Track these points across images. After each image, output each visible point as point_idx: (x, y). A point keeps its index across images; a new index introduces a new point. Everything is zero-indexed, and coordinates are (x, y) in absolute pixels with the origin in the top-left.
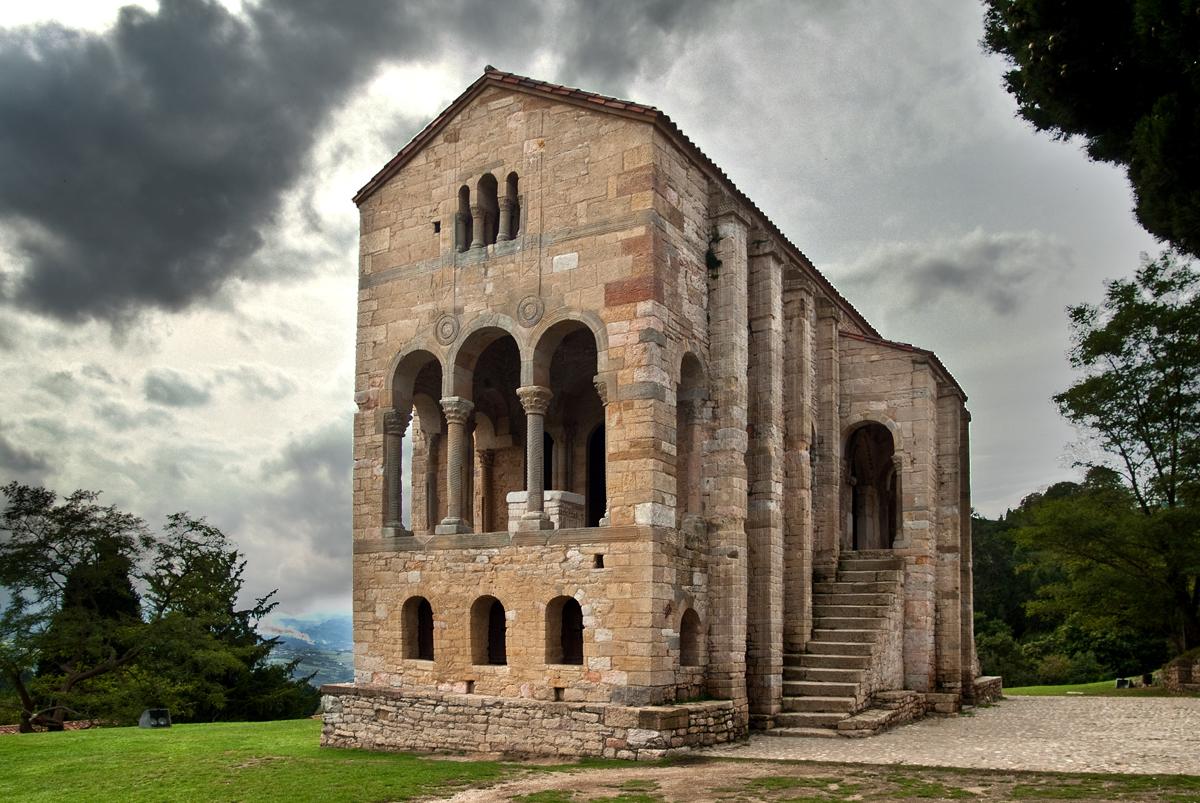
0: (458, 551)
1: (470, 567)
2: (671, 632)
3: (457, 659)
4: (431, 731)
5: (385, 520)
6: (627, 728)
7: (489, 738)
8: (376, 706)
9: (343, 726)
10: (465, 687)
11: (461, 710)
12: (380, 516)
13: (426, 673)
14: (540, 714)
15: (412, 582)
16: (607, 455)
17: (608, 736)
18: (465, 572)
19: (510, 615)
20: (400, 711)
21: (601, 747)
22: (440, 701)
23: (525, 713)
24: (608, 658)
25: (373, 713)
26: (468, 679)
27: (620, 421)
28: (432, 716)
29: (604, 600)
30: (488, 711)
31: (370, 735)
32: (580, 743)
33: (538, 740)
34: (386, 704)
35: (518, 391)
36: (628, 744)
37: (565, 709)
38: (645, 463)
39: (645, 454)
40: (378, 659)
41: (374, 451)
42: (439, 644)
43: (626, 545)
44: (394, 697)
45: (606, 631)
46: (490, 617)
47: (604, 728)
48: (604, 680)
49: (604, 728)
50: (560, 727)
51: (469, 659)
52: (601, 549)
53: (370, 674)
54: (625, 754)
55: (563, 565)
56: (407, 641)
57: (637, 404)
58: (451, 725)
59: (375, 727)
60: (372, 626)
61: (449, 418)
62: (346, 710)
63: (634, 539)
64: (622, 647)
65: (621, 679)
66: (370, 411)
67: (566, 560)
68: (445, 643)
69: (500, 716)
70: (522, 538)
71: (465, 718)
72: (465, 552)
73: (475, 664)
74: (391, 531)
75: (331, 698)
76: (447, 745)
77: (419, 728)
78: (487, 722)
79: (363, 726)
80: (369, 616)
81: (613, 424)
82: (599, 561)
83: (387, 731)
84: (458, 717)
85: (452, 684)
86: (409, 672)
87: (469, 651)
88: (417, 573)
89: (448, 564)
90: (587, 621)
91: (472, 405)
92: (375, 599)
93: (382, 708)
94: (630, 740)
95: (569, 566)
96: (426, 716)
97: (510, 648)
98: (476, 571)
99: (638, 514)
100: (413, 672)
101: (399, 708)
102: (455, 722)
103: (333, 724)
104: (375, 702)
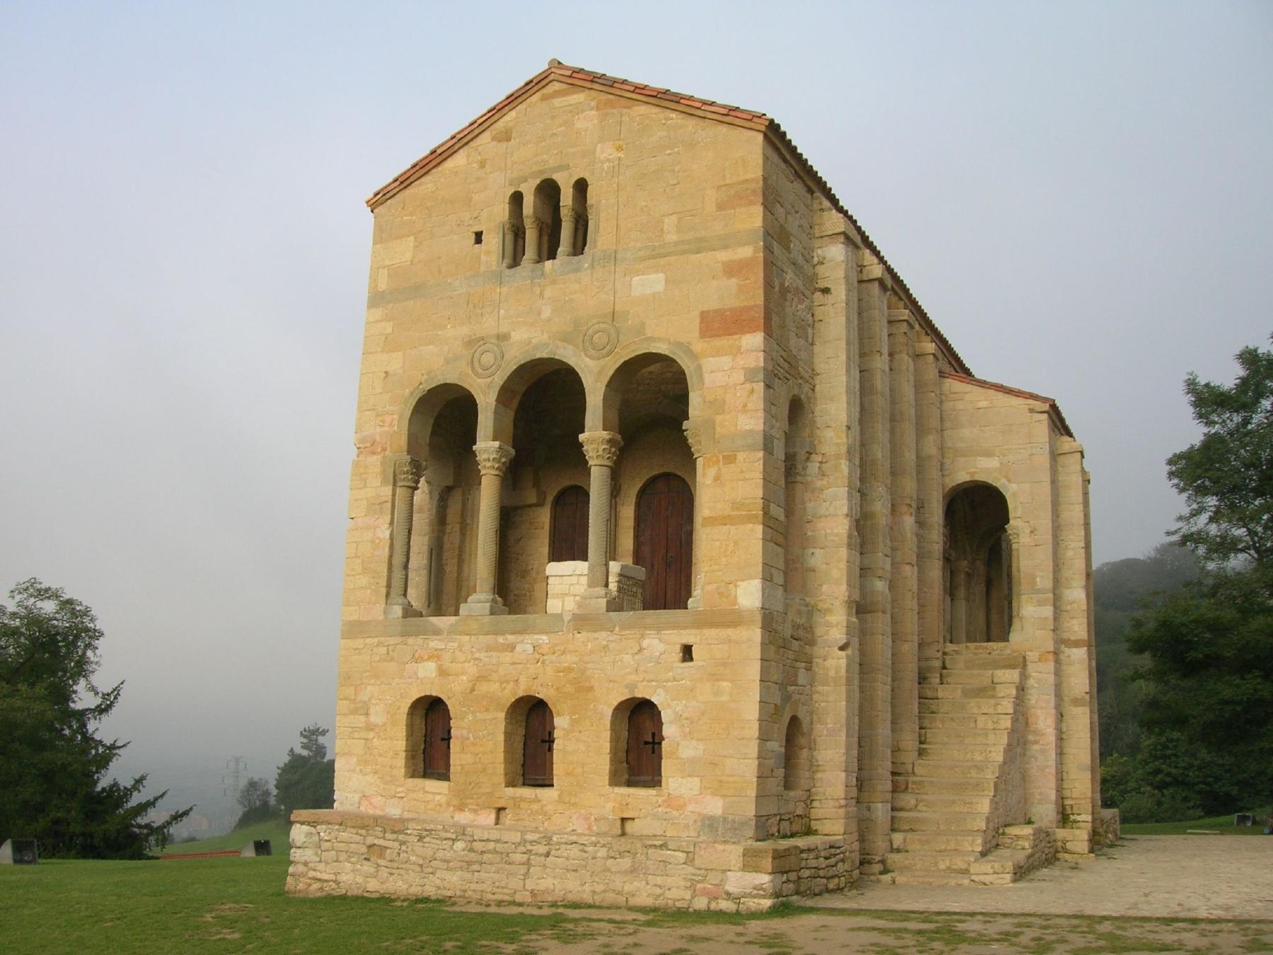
0: (490, 639)
1: (507, 657)
2: (777, 746)
5: (388, 595)
6: (724, 871)
7: (530, 884)
8: (370, 840)
9: (321, 866)
10: (493, 816)
11: (491, 846)
12: (384, 590)
13: (438, 797)
14: (602, 852)
15: (425, 679)
16: (698, 520)
17: (699, 882)
18: (499, 664)
19: (561, 723)
20: (404, 848)
21: (688, 897)
22: (462, 832)
23: (582, 851)
24: (697, 780)
25: (364, 849)
26: (499, 806)
27: (717, 478)
28: (449, 855)
29: (695, 703)
30: (530, 848)
31: (359, 880)
32: (659, 891)
33: (600, 888)
34: (384, 838)
35: (581, 437)
36: (728, 894)
37: (639, 845)
38: (752, 530)
39: (750, 519)
40: (369, 778)
41: (377, 507)
42: (458, 757)
44: (396, 827)
45: (694, 743)
46: (532, 724)
47: (694, 871)
48: (690, 808)
49: (694, 871)
50: (633, 870)
51: (501, 779)
52: (688, 637)
53: (357, 797)
54: (725, 905)
55: (636, 657)
56: (411, 755)
57: (741, 456)
58: (476, 867)
59: (368, 868)
60: (364, 735)
61: (485, 467)
62: (326, 845)
64: (716, 765)
65: (715, 806)
66: (375, 457)
68: (468, 759)
69: (548, 855)
71: (497, 858)
72: (501, 640)
73: (511, 784)
74: (398, 611)
75: (305, 828)
76: (470, 893)
77: (430, 870)
78: (528, 863)
81: (709, 481)
83: (384, 873)
84: (485, 856)
85: (475, 811)
86: (414, 796)
87: (501, 769)
88: (431, 666)
89: (477, 655)
90: (667, 730)
91: (513, 452)
93: (376, 842)
94: (729, 888)
95: (642, 656)
96: (440, 854)
97: (558, 769)
98: (514, 663)
99: (740, 592)
100: (421, 795)
101: (403, 843)
103: (306, 864)
104: (369, 835)
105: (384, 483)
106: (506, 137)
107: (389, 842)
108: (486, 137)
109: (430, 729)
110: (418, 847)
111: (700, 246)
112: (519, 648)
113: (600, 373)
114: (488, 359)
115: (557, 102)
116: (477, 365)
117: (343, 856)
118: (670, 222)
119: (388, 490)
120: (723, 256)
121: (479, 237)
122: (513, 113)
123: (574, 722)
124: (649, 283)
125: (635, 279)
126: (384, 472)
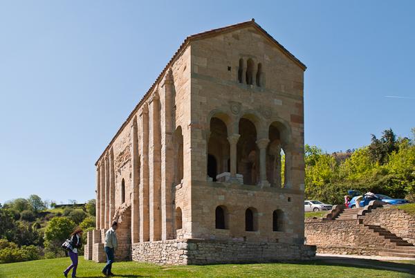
0: (241, 191)
1: (246, 196)
4: (241, 255)
7: (263, 256)
15: (221, 200)
19: (261, 214)
31: (214, 258)
43: (298, 196)
50: (288, 251)
51: (244, 229)
52: (290, 196)
54: (307, 259)
59: (216, 255)
70: (265, 189)
79: (209, 255)
82: (289, 200)
94: (309, 254)
103: (194, 255)
105: (204, 139)
107: (223, 246)
113: (268, 123)
114: (236, 109)
118: (282, 86)
119: (205, 142)
120: (295, 101)
123: (264, 215)
124: (278, 102)
125: (275, 100)
126: (203, 135)
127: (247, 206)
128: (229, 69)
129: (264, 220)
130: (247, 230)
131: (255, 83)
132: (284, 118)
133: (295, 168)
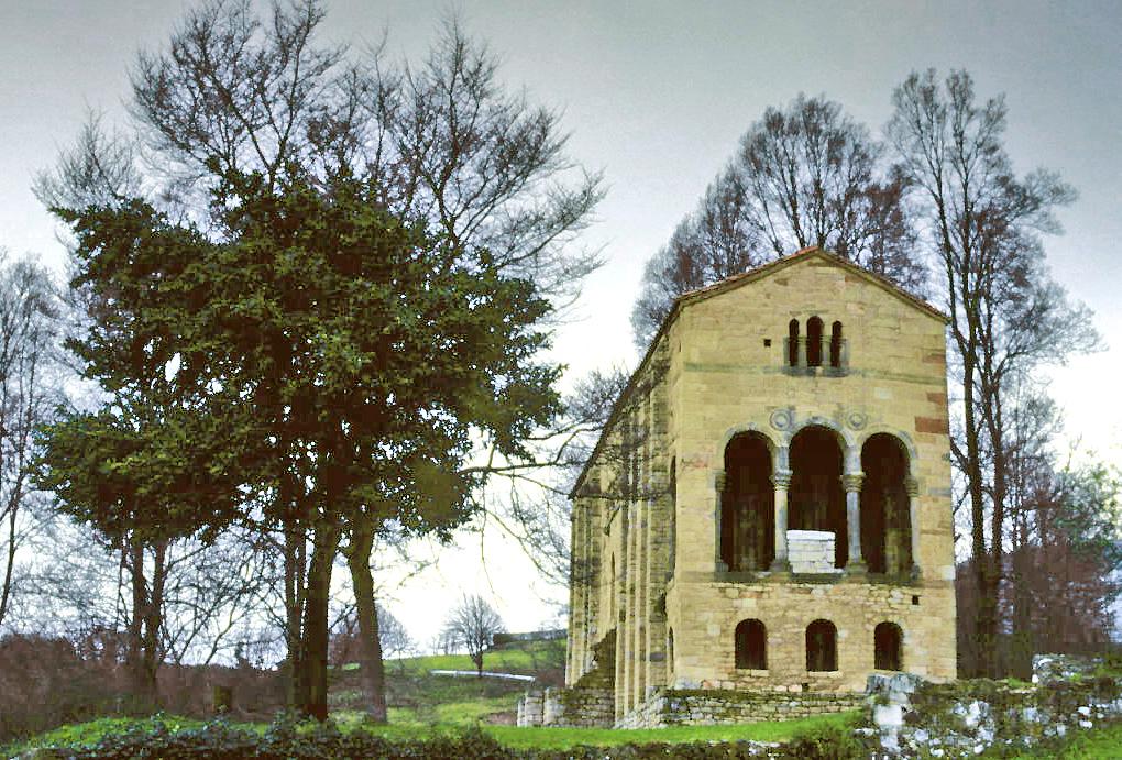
0: (795, 585)
1: (808, 597)
3: (792, 666)
8: (729, 704)
15: (749, 608)
19: (842, 634)
40: (709, 669)
42: (773, 655)
44: (747, 697)
52: (917, 592)
55: (889, 600)
60: (703, 642)
63: (942, 588)
67: (891, 596)
68: (782, 655)
72: (802, 586)
80: (701, 634)
82: (915, 600)
84: (813, 709)
87: (804, 661)
90: (906, 641)
92: (707, 621)
102: (809, 713)
106: (784, 282)
108: (771, 279)
109: (751, 642)
110: (765, 708)
111: (910, 378)
112: (813, 591)
114: (782, 420)
115: (820, 269)
116: (774, 424)
117: (710, 716)
121: (767, 343)
122: (788, 269)
127: (808, 618)
128: (767, 343)
129: (855, 650)
130: (811, 666)
131: (826, 362)
132: (897, 424)
133: (926, 532)
